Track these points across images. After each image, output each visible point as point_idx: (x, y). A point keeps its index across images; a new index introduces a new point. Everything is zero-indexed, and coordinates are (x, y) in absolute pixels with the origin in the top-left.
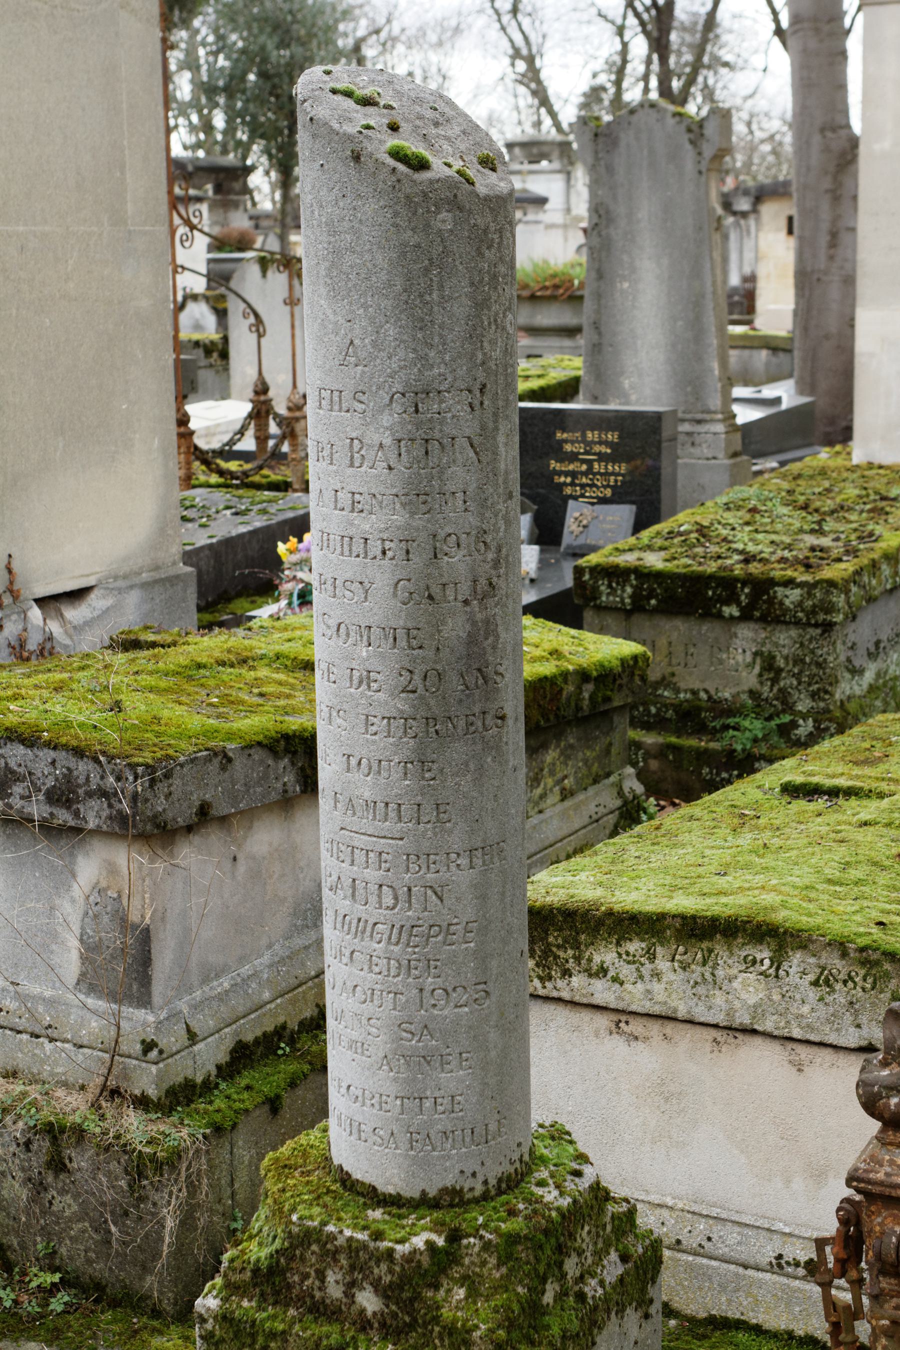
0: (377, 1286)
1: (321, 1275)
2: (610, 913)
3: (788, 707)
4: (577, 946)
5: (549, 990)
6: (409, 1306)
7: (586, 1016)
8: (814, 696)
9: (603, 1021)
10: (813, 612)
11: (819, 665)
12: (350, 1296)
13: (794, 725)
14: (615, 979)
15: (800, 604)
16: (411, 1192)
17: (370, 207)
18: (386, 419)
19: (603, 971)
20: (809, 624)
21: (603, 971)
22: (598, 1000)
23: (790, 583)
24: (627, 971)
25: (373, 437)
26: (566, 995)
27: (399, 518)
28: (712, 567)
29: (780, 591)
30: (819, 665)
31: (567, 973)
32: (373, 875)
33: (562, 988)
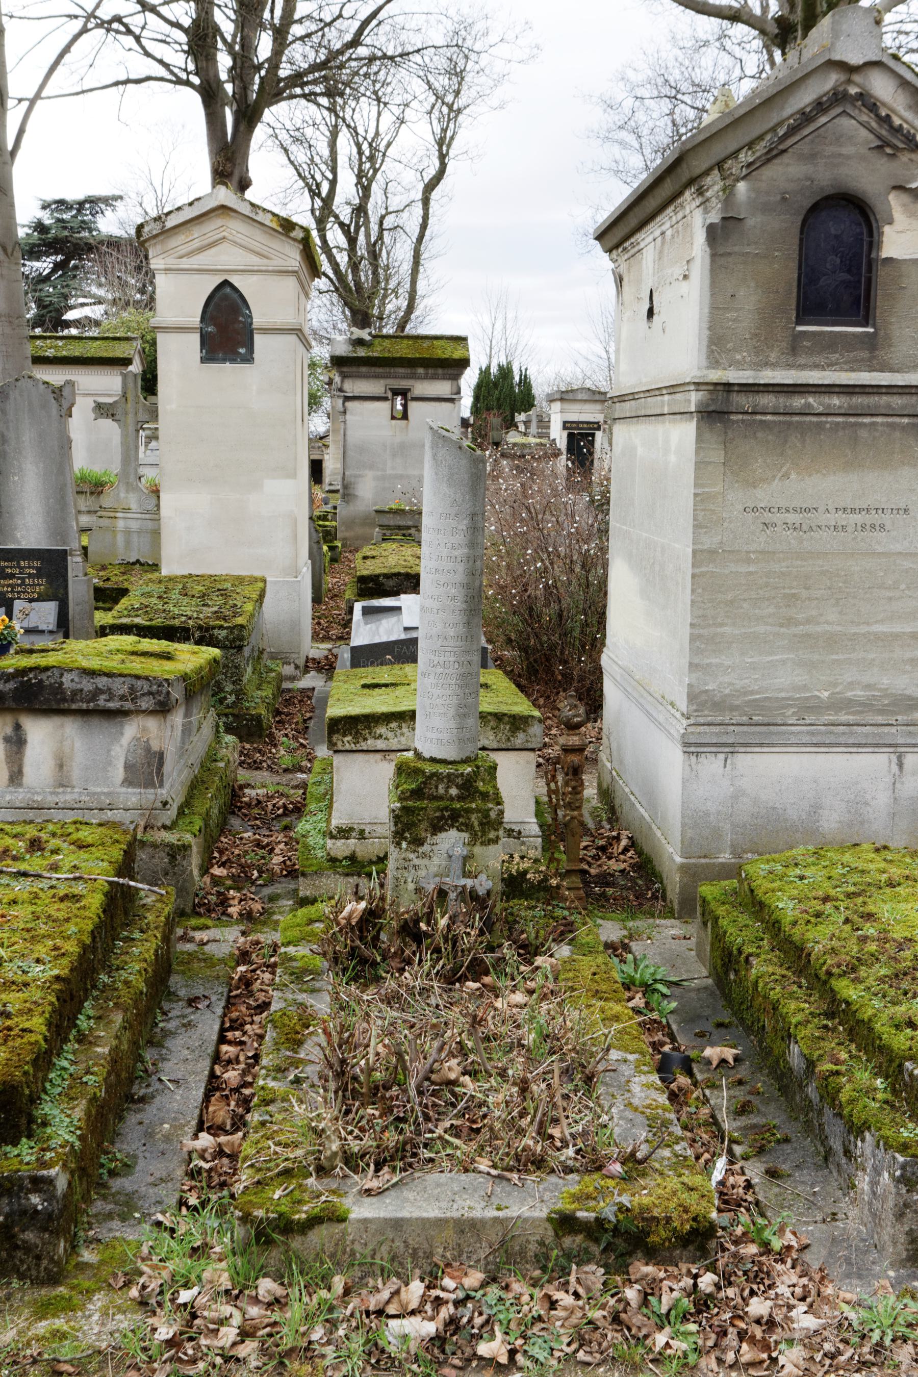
0: (457, 786)
1: (437, 787)
2: (383, 714)
3: (221, 690)
4: (369, 728)
5: (358, 747)
6: (468, 790)
7: (371, 756)
8: (234, 683)
9: (378, 756)
10: (234, 640)
11: (236, 667)
12: (447, 791)
13: (225, 698)
14: (386, 739)
15: (227, 637)
16: (458, 759)
17: (464, 462)
18: (465, 522)
19: (381, 736)
20: (231, 647)
21: (381, 736)
22: (379, 748)
23: (221, 627)
24: (390, 735)
25: (460, 527)
26: (365, 748)
27: (466, 551)
28: (177, 622)
29: (216, 632)
30: (236, 667)
31: (365, 739)
32: (452, 659)
33: (364, 746)
